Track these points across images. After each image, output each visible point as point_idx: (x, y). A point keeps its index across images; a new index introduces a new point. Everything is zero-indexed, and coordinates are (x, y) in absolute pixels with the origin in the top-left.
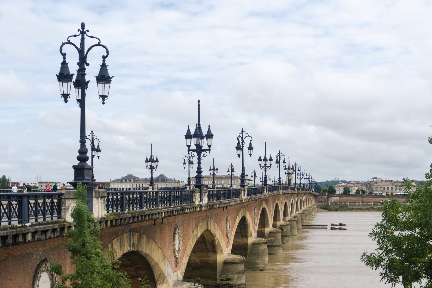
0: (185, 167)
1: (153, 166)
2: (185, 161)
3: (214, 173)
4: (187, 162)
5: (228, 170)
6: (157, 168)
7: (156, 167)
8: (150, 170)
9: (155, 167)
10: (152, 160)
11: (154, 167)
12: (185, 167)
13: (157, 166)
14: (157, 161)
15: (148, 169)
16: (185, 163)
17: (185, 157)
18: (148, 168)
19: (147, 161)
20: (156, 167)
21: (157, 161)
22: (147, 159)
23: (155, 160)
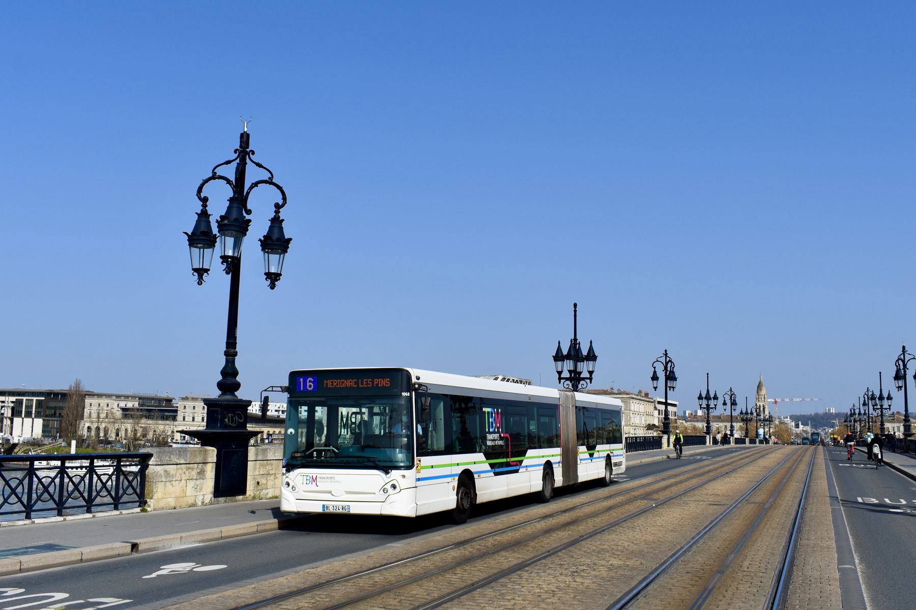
0: (655, 388)
1: (580, 373)
2: (655, 372)
3: (708, 405)
4: (661, 375)
5: (725, 401)
6: (591, 379)
7: (588, 376)
8: (571, 384)
9: (585, 374)
10: (575, 354)
11: (582, 376)
12: (655, 388)
13: (591, 373)
14: (591, 356)
15: (562, 381)
16: (655, 378)
17: (657, 361)
18: (563, 378)
19: (559, 357)
20: (588, 376)
21: (591, 356)
22: (559, 349)
23: (585, 352)
